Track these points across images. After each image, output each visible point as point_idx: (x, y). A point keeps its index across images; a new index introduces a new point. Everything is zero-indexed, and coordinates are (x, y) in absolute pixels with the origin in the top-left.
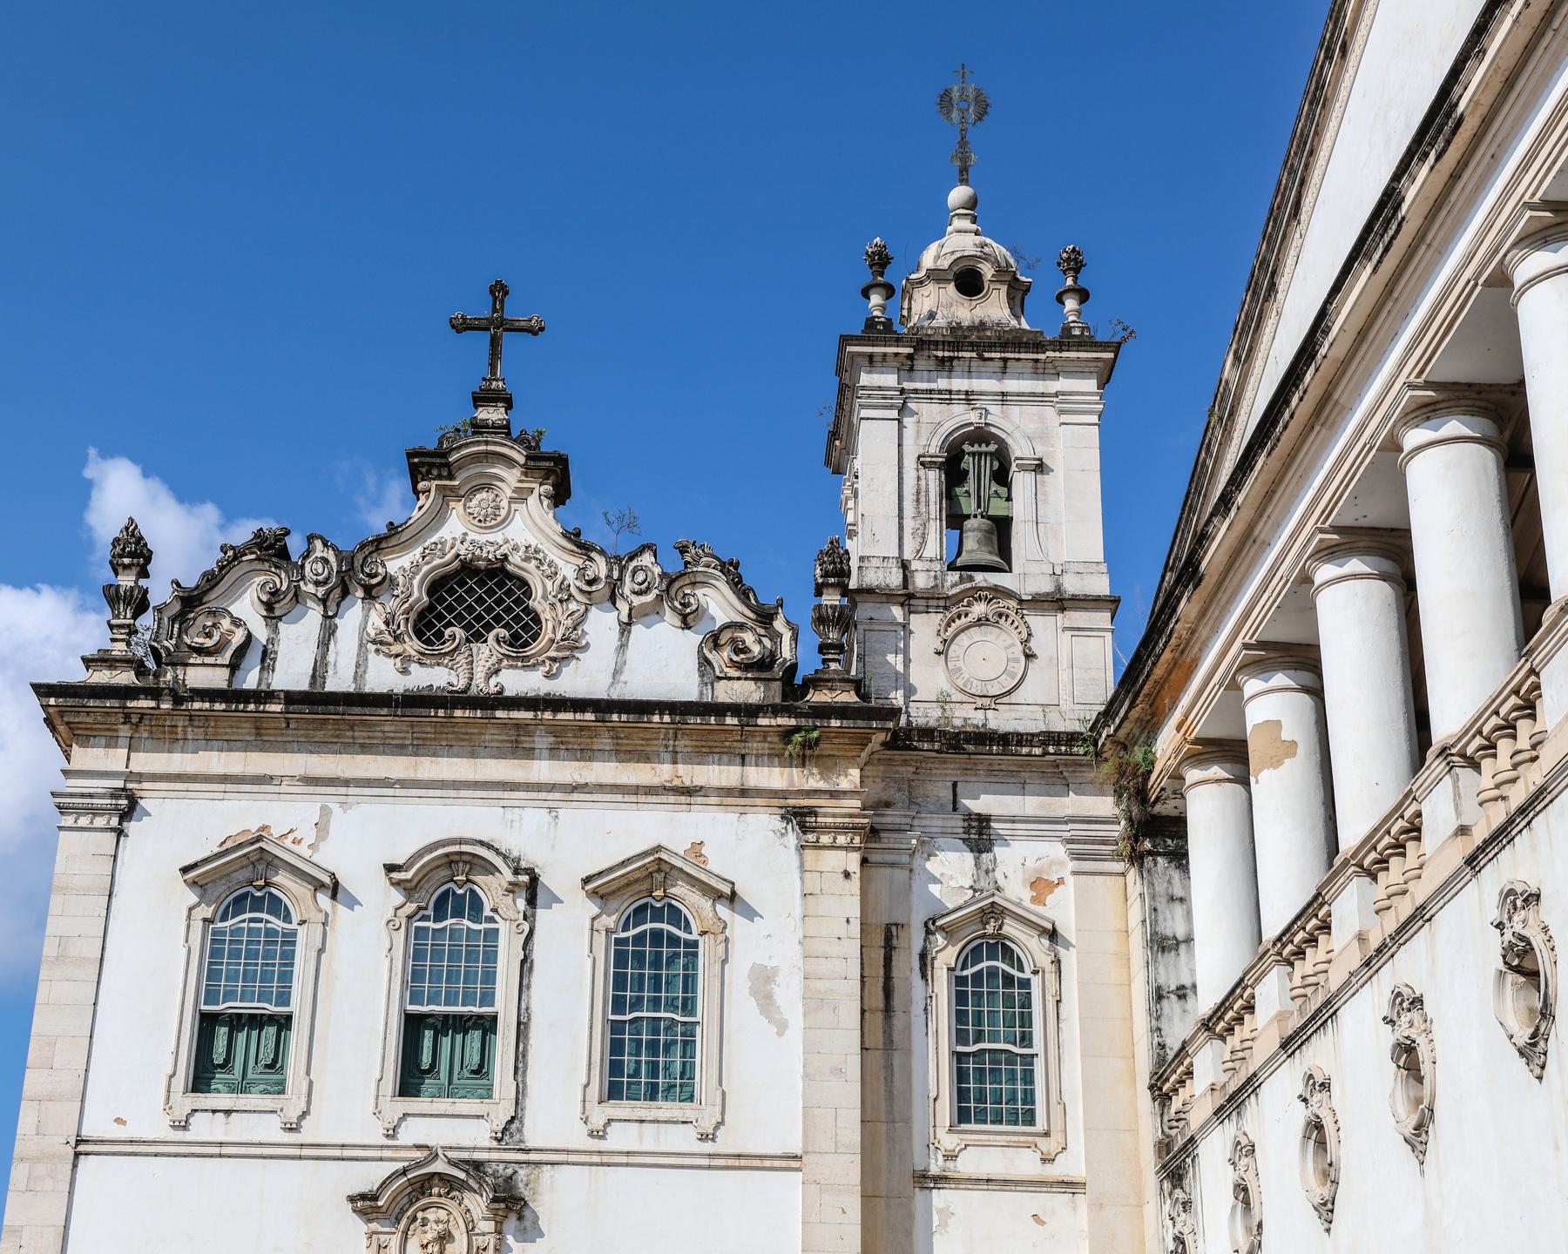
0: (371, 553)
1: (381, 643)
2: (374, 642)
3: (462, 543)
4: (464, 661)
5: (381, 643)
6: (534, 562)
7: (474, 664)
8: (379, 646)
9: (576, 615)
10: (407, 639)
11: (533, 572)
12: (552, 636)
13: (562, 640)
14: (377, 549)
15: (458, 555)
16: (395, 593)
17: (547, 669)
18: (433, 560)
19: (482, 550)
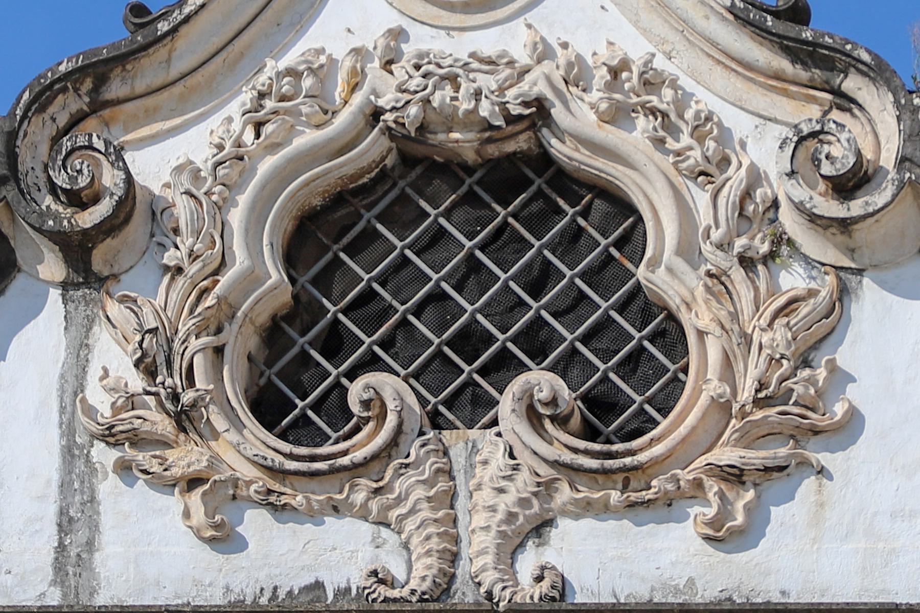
0: (76, 120)
1: (137, 440)
2: (110, 436)
3: (387, 65)
4: (420, 492)
5: (137, 440)
6: (642, 122)
7: (461, 503)
8: (129, 452)
9: (804, 309)
10: (220, 423)
11: (638, 158)
12: (714, 387)
13: (759, 403)
14: (97, 106)
15: (376, 114)
16: (170, 257)
17: (711, 512)
18: (291, 133)
19: (457, 89)
